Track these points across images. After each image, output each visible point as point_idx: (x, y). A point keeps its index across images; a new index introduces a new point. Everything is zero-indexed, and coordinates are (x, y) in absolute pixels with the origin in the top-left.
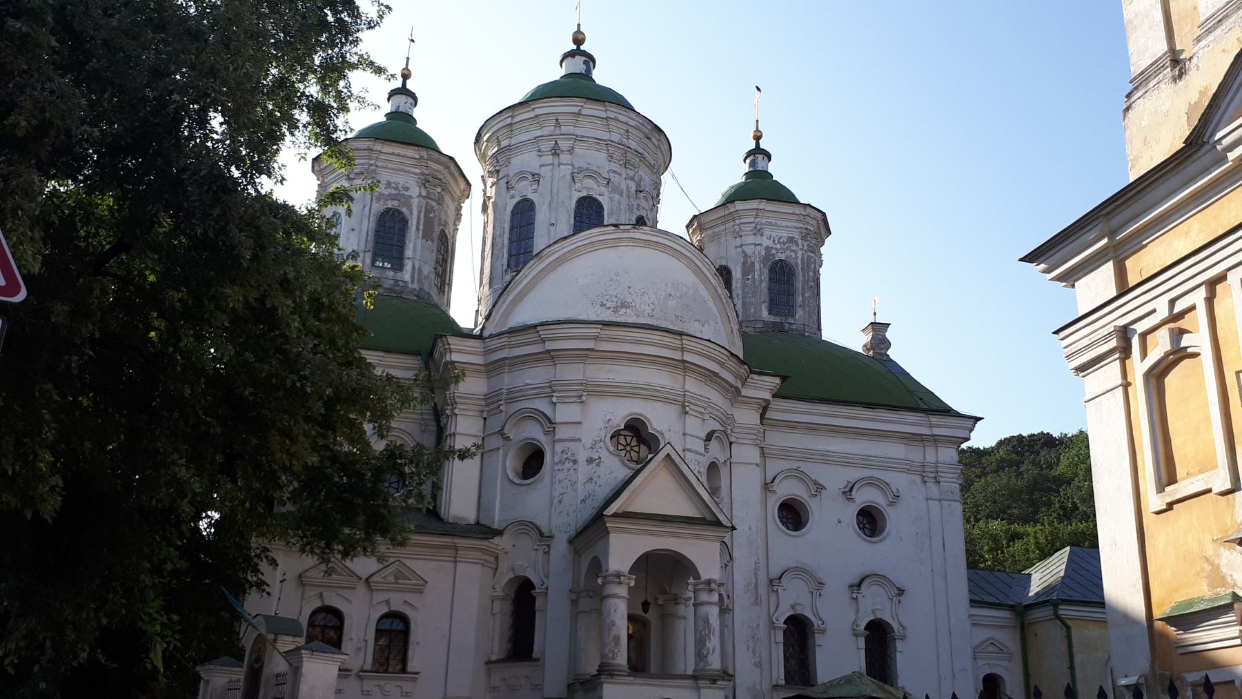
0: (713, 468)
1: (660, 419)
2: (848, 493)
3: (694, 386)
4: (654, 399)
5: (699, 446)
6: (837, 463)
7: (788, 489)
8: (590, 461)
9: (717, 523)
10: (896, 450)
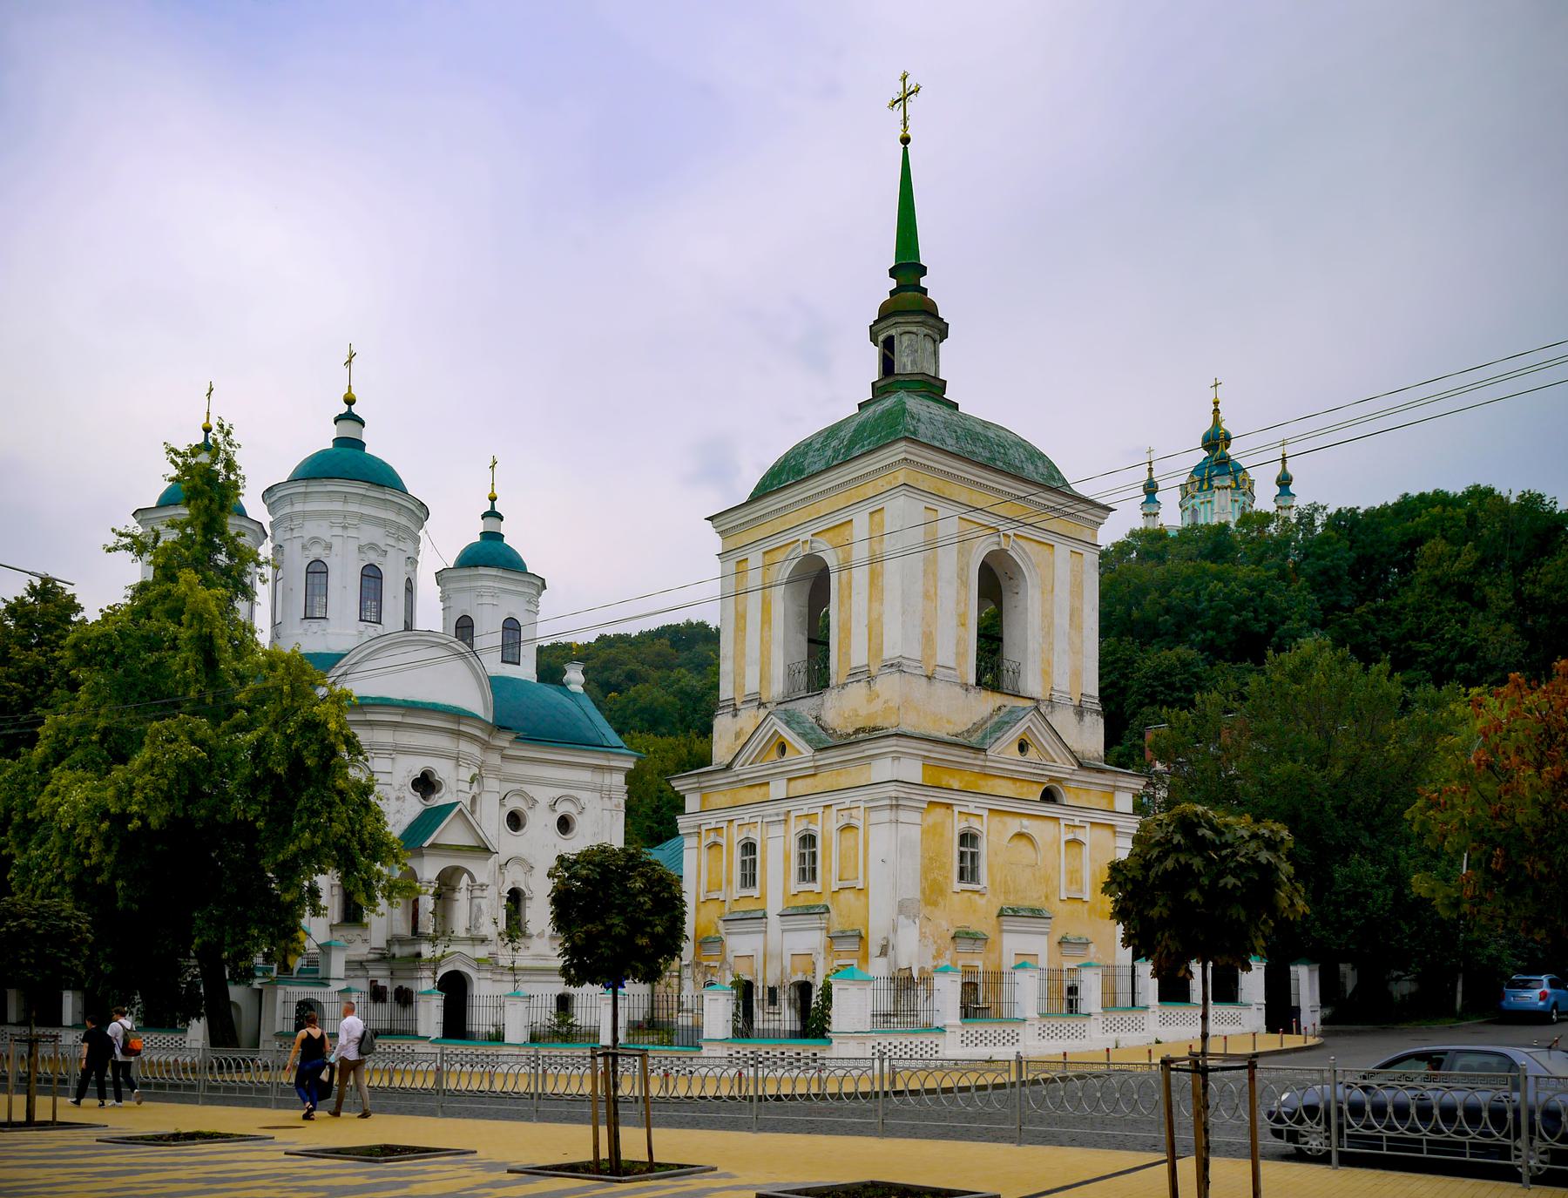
0: (474, 799)
1: (443, 770)
2: (552, 807)
3: (465, 747)
4: (441, 756)
5: (466, 787)
6: (547, 785)
7: (514, 804)
8: (398, 799)
9: (487, 850)
10: (586, 776)
